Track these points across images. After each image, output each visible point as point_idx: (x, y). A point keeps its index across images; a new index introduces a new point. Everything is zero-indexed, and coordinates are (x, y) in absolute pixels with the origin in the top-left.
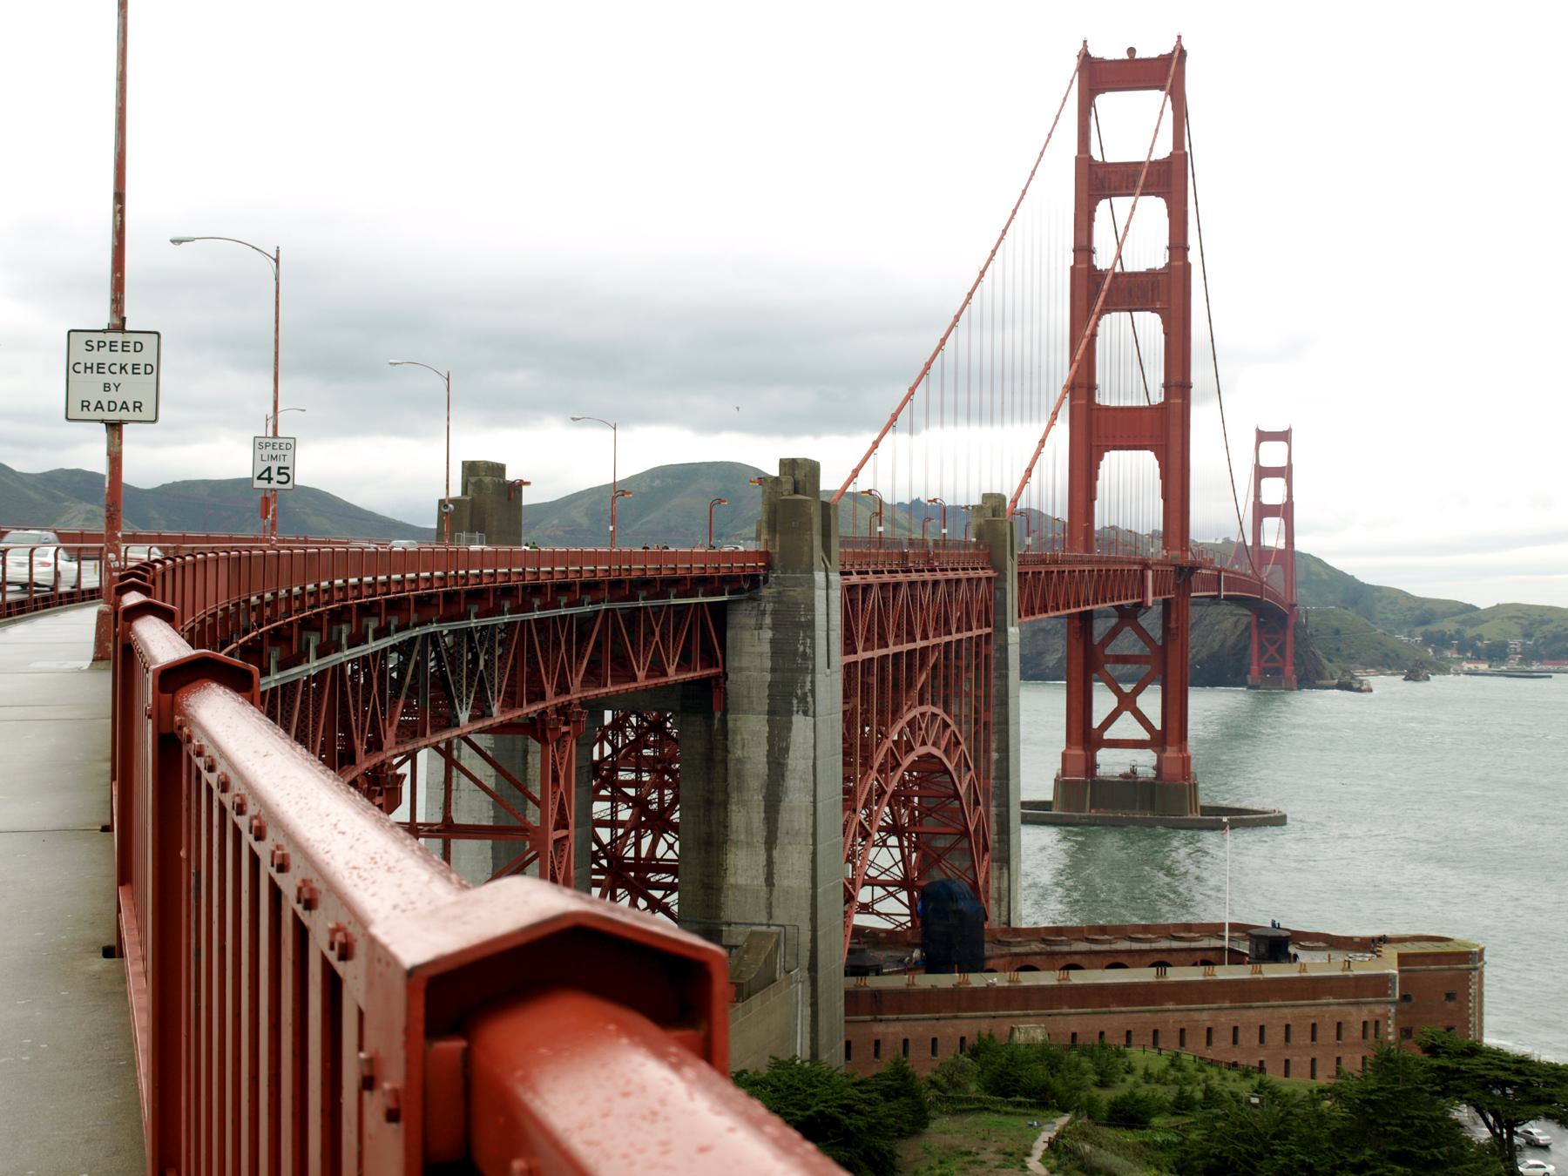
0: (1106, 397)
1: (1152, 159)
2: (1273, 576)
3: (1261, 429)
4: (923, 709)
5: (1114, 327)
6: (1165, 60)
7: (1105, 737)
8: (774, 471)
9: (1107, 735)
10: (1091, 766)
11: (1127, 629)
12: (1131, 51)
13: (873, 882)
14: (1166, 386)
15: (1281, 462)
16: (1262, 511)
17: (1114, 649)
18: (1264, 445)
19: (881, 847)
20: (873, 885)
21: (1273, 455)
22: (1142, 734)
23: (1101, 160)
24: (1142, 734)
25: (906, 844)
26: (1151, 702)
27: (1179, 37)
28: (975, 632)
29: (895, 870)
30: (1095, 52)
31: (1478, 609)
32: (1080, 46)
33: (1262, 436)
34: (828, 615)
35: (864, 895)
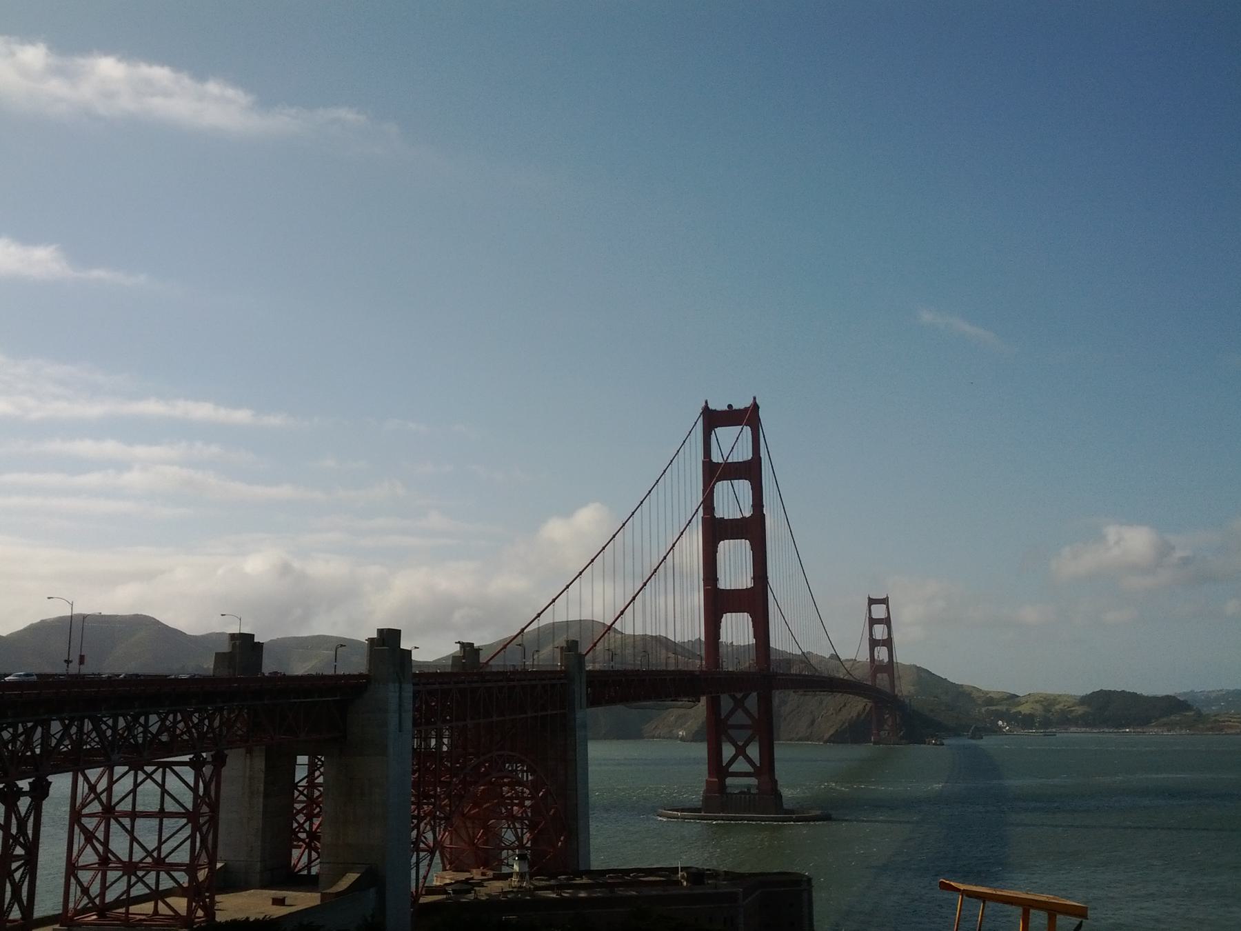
0: (725, 583)
1: (730, 460)
2: (882, 680)
3: (872, 597)
4: (499, 753)
5: (725, 547)
6: (746, 409)
7: (730, 771)
8: (375, 635)
9: (731, 770)
10: (722, 787)
11: (740, 710)
12: (730, 406)
13: (507, 848)
14: (754, 578)
15: (883, 615)
16: (874, 643)
17: (731, 721)
18: (873, 606)
19: (507, 828)
20: (508, 849)
21: (879, 611)
22: (748, 768)
23: (721, 461)
24: (748, 768)
25: (517, 825)
26: (753, 751)
27: (755, 398)
28: (549, 712)
29: (516, 842)
30: (712, 407)
31: (1018, 696)
32: (704, 404)
33: (872, 602)
34: (400, 706)
35: (504, 853)
